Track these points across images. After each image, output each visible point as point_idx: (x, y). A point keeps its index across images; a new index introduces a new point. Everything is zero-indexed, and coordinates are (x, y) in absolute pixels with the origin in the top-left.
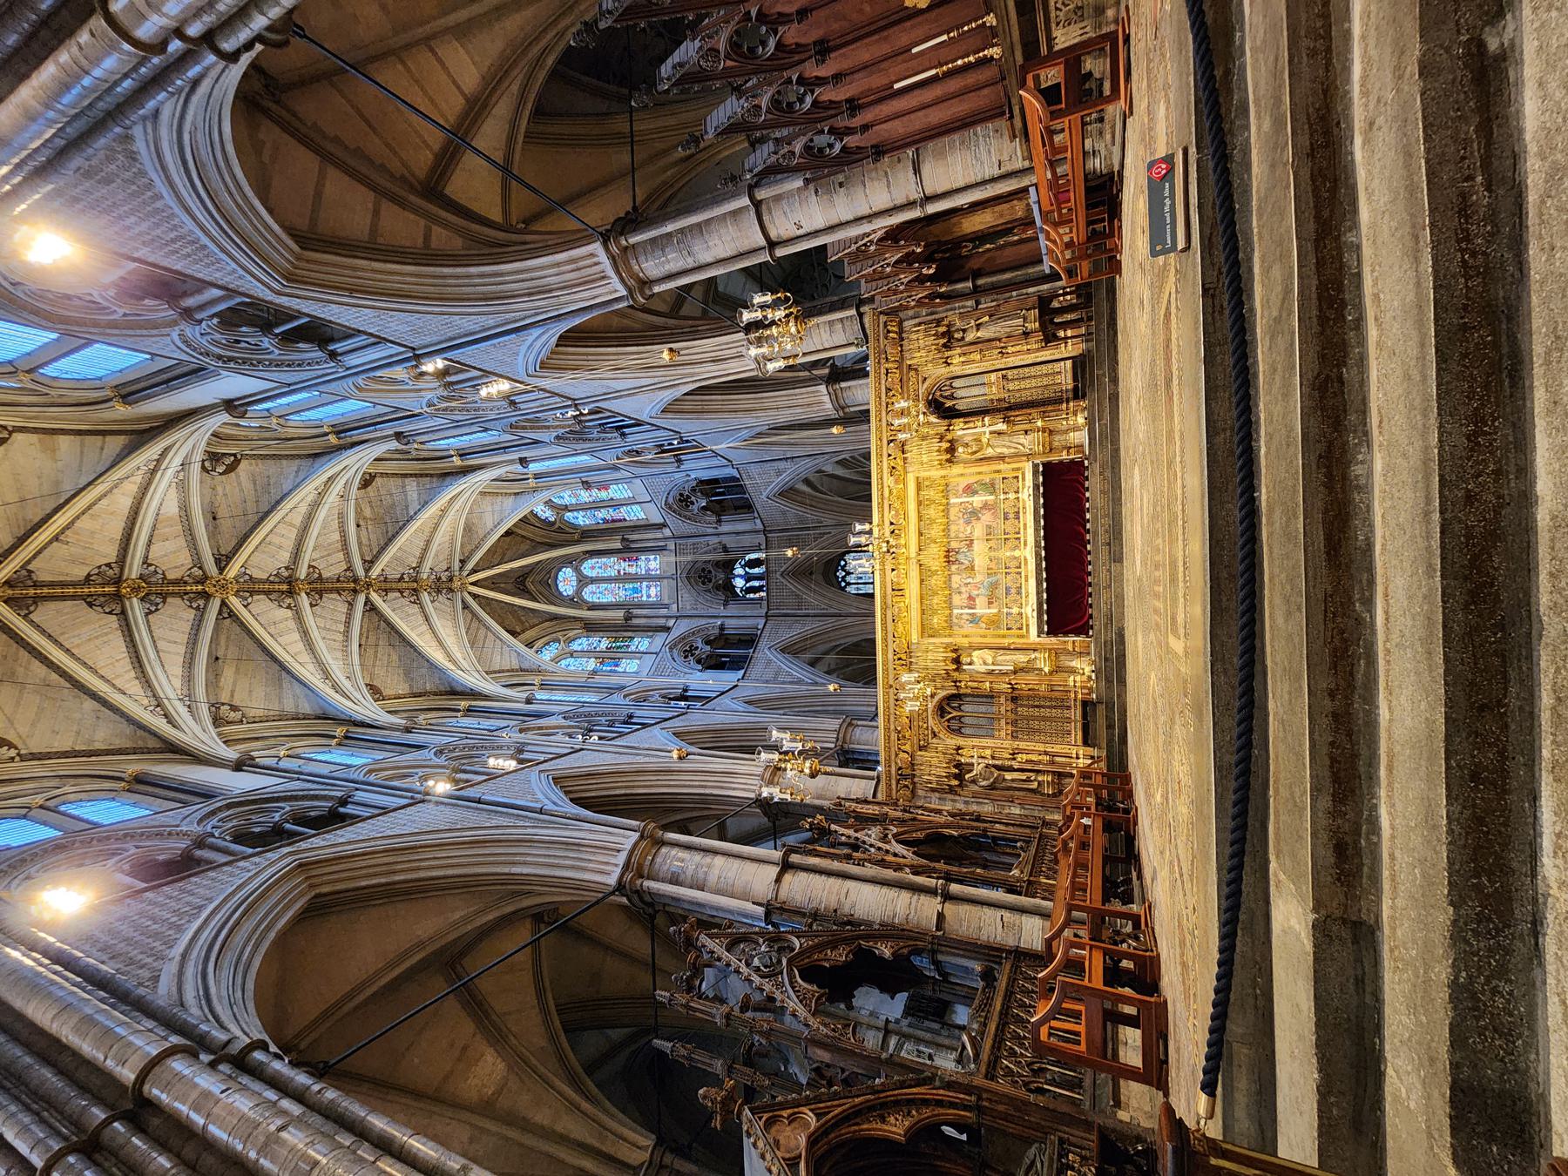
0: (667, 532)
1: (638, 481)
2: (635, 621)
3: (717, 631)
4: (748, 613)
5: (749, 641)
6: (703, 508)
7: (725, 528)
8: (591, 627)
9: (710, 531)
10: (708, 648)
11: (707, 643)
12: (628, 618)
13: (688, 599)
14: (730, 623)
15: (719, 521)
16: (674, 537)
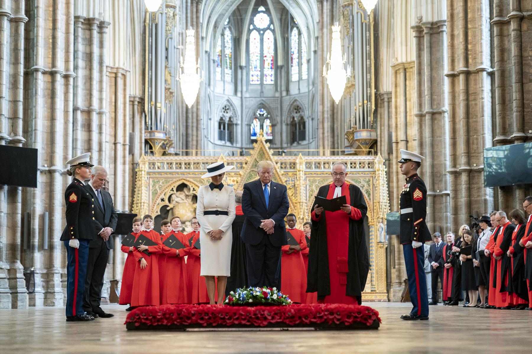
0: (284, 94)
1: (307, 90)
2: (239, 71)
3: (235, 122)
4: (244, 137)
5: (231, 139)
6: (294, 118)
7: (284, 127)
8: (237, 42)
9: (283, 118)
10: (227, 119)
11: (230, 118)
12: (241, 68)
13: (251, 103)
14: (239, 127)
15: (287, 125)
16: (282, 97)
